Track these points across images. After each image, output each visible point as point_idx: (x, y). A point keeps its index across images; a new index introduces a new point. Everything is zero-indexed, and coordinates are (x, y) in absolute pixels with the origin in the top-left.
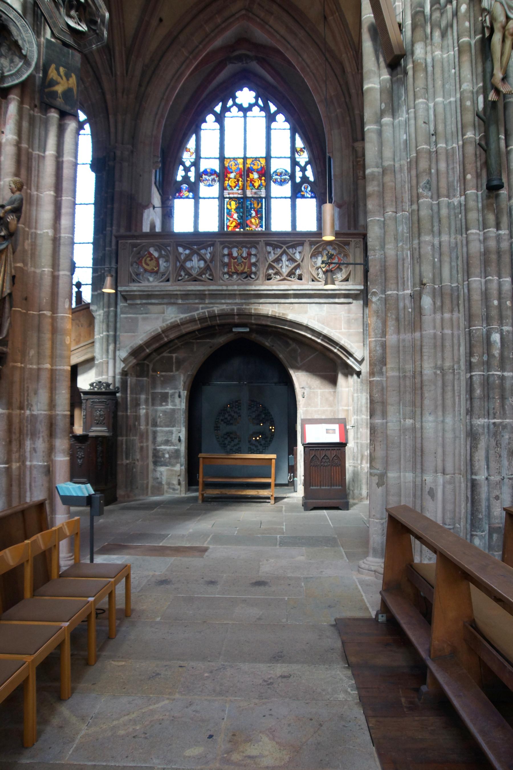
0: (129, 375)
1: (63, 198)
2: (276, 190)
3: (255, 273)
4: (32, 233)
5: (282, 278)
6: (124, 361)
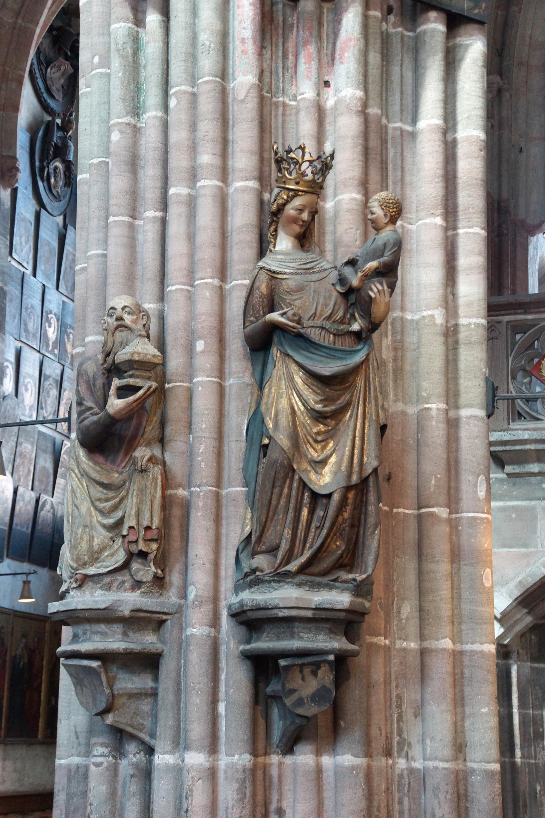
0: (514, 656)
1: (461, 231)
4: (394, 319)
6: (504, 619)
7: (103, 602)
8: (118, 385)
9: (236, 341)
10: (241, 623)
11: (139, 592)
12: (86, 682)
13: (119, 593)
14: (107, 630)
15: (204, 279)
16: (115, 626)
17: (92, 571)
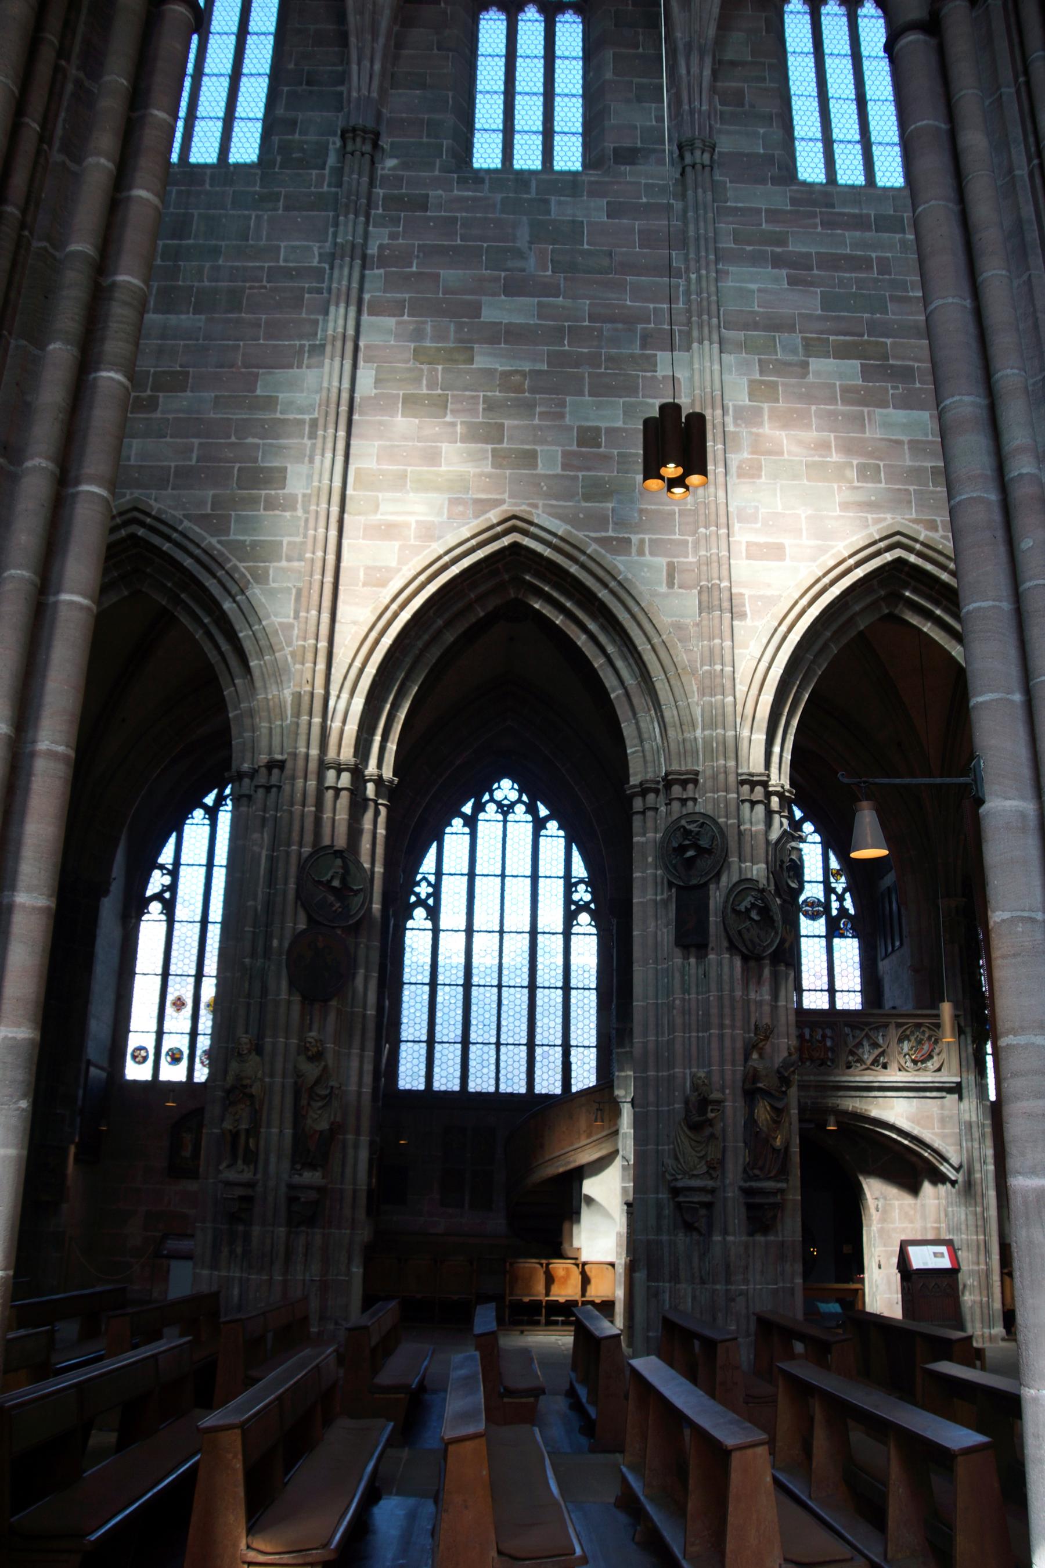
2: (807, 926)
3: (833, 1061)
5: (864, 1067)
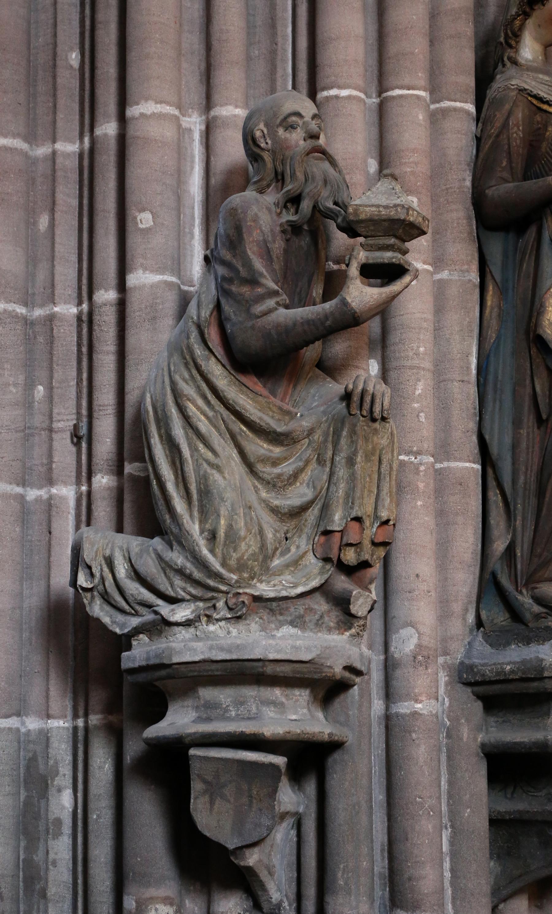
7: (308, 649)
8: (364, 261)
9: (454, 207)
10: (479, 697)
11: (347, 634)
12: (229, 791)
13: (320, 634)
14: (284, 700)
15: (413, 88)
16: (297, 692)
17: (265, 589)
